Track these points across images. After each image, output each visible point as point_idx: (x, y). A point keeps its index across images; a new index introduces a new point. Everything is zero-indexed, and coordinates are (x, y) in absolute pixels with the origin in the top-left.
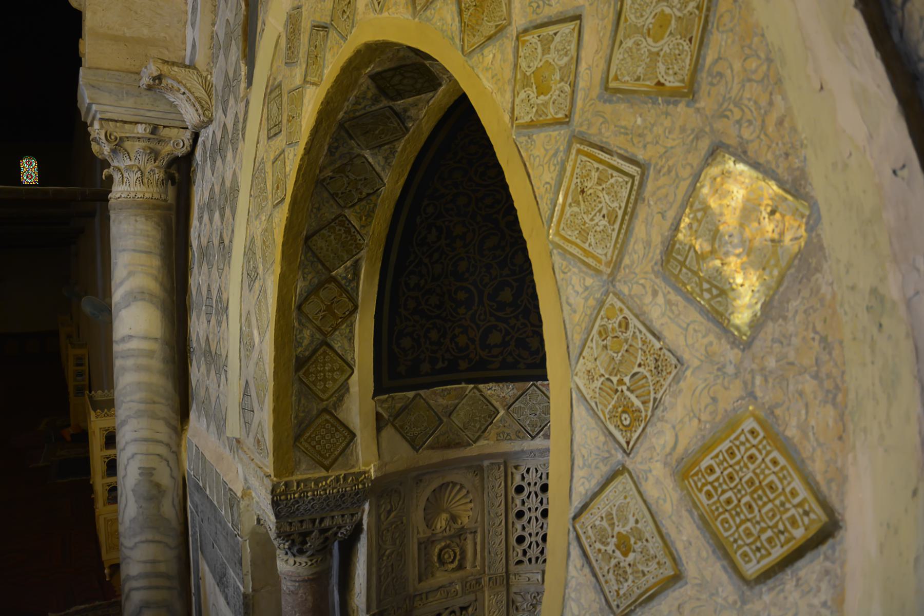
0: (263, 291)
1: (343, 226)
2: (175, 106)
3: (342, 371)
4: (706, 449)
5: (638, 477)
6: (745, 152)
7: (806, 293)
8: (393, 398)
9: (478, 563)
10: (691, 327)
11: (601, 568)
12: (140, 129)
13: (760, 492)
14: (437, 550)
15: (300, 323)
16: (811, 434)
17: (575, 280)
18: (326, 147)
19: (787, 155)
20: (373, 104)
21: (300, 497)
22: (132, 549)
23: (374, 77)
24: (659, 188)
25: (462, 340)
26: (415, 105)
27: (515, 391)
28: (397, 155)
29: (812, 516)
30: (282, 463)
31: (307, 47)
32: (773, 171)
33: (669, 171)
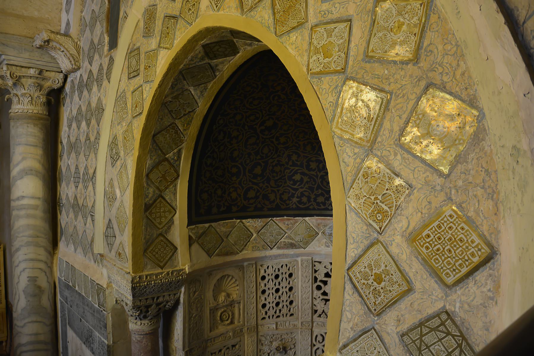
0: (124, 166)
1: (174, 129)
2: (55, 59)
3: (170, 212)
4: (425, 226)
5: (387, 244)
6: (445, 87)
7: (477, 150)
8: (198, 227)
9: (241, 320)
10: (416, 169)
11: (364, 292)
12: (32, 72)
13: (455, 243)
14: (219, 314)
15: (147, 184)
16: (481, 214)
17: (348, 150)
18: (170, 84)
19: (466, 89)
20: (200, 61)
21: (147, 284)
22: (22, 327)
23: (204, 46)
24: (397, 104)
25: (234, 195)
26: (222, 63)
27: (262, 223)
28: (207, 90)
29: (483, 251)
30: (137, 266)
31: (161, 28)
32: (460, 96)
33: (403, 96)
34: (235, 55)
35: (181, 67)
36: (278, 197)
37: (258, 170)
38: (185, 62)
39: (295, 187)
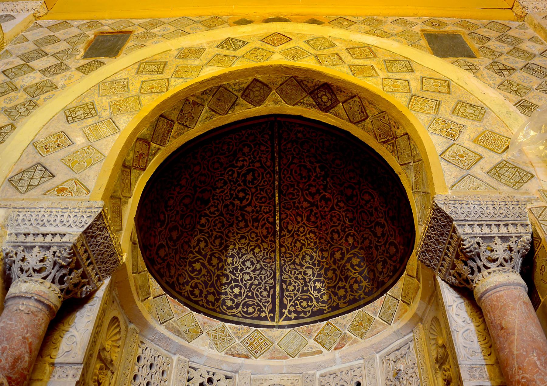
18: (206, 89)
23: (255, 80)
34: (256, 106)
35: (225, 83)
36: (177, 276)
37: (175, 235)
38: (229, 82)
39: (192, 275)
